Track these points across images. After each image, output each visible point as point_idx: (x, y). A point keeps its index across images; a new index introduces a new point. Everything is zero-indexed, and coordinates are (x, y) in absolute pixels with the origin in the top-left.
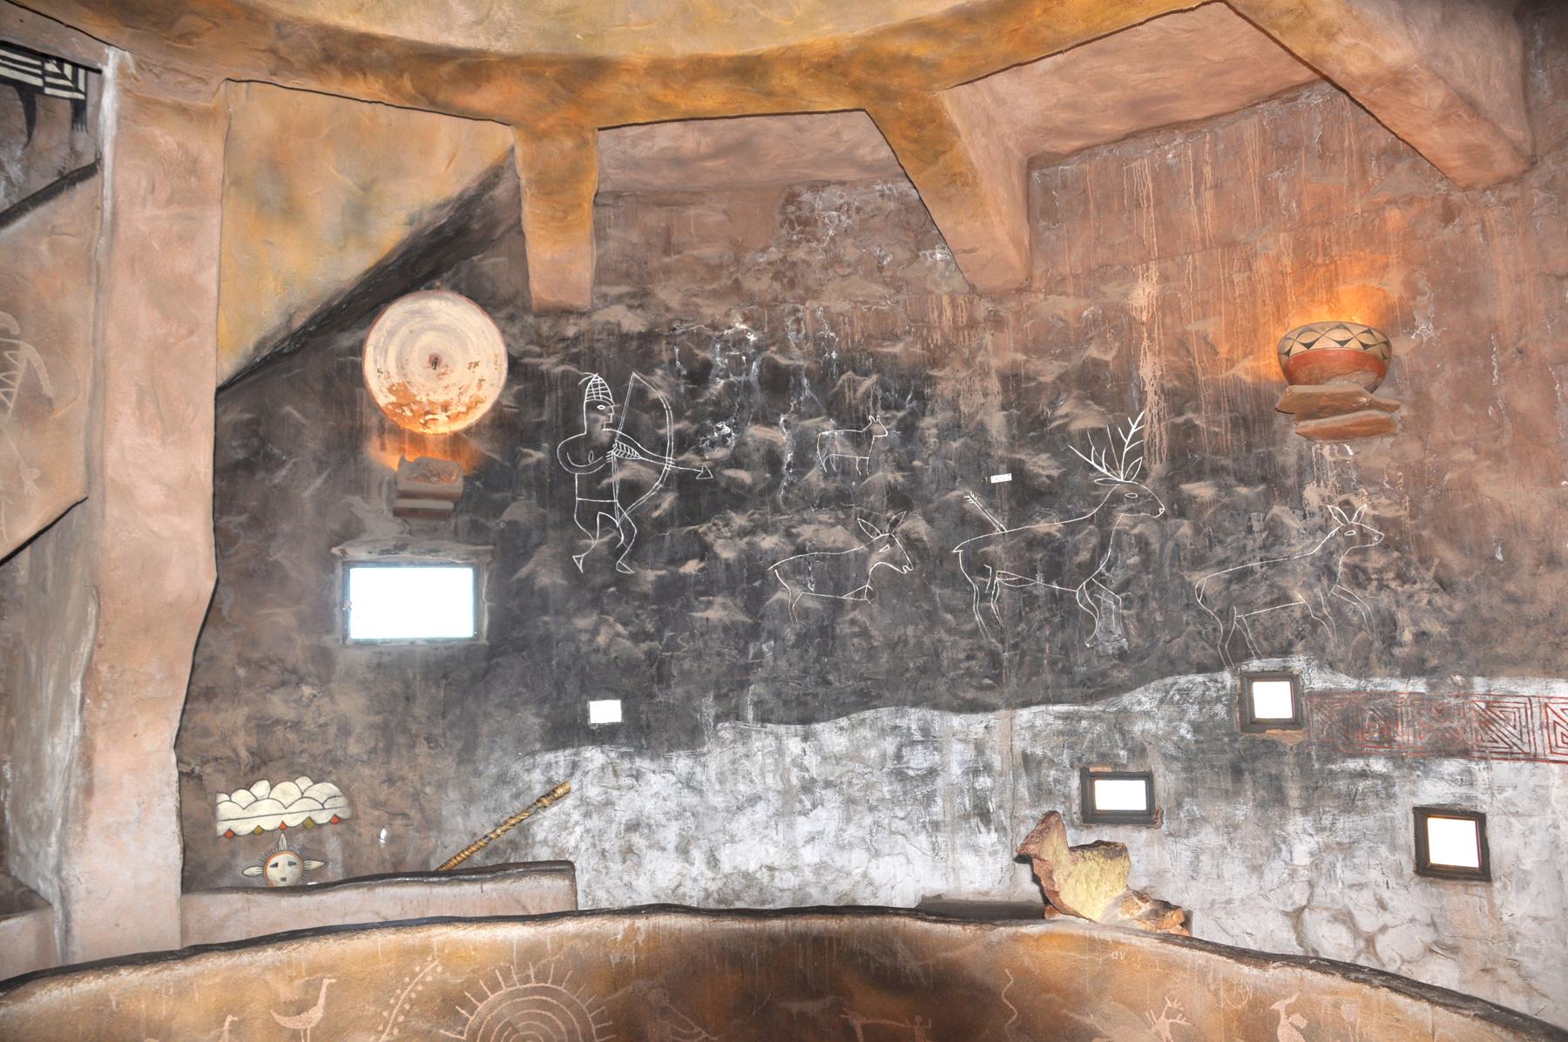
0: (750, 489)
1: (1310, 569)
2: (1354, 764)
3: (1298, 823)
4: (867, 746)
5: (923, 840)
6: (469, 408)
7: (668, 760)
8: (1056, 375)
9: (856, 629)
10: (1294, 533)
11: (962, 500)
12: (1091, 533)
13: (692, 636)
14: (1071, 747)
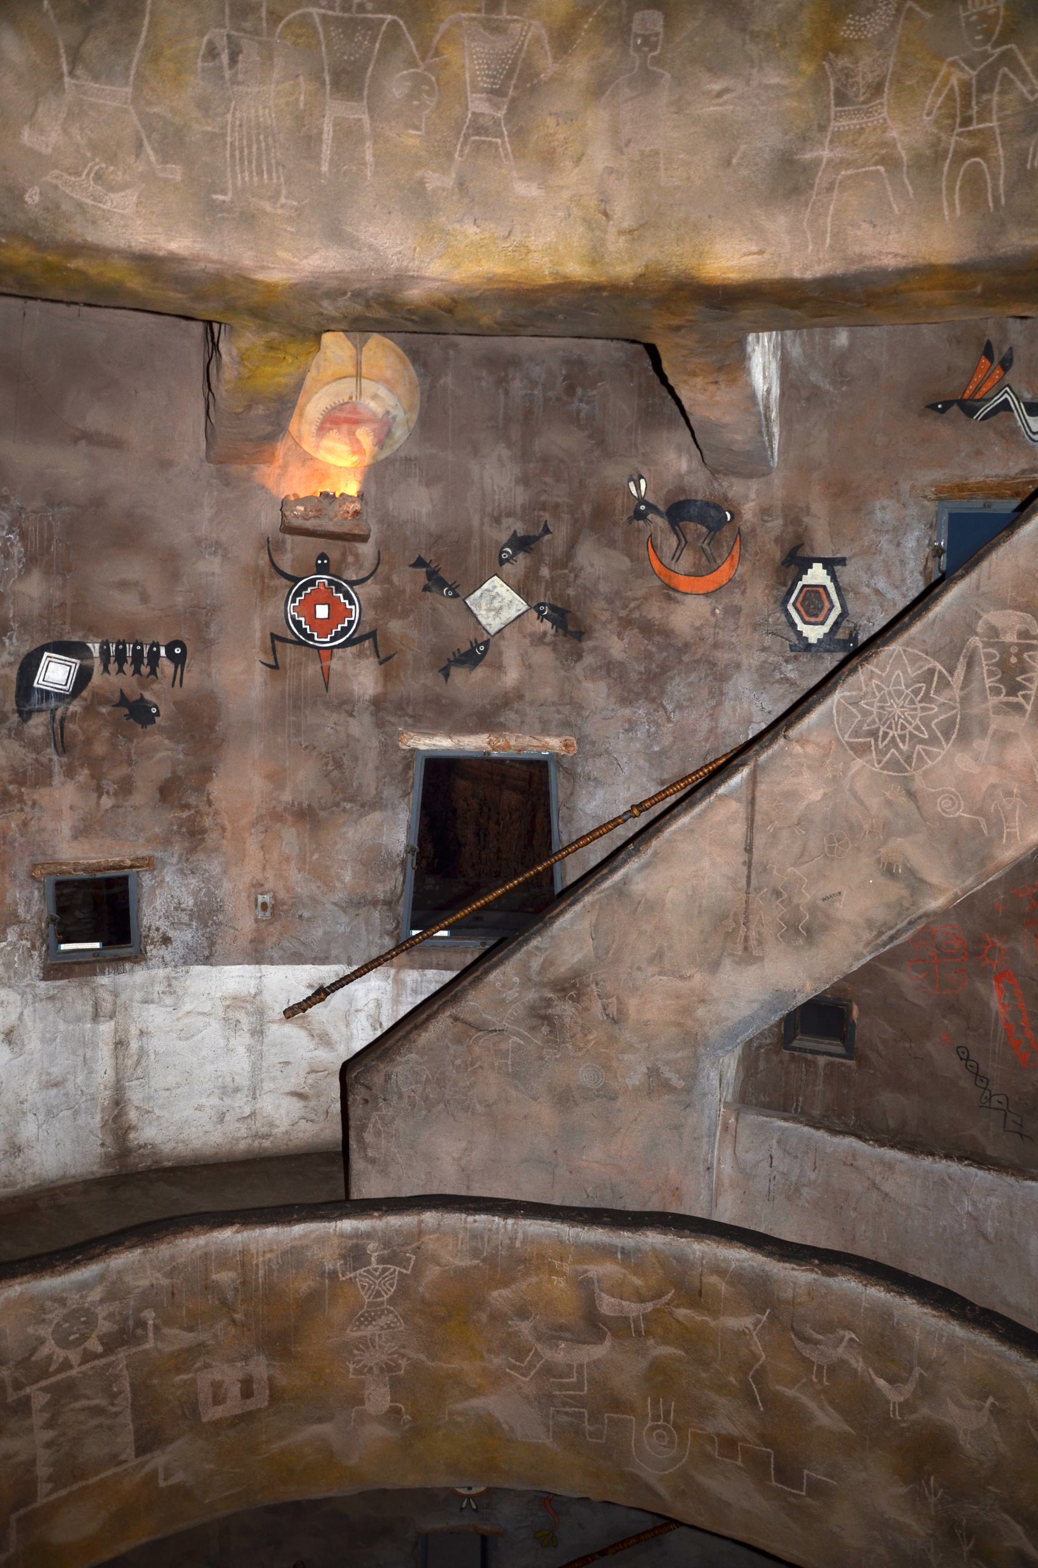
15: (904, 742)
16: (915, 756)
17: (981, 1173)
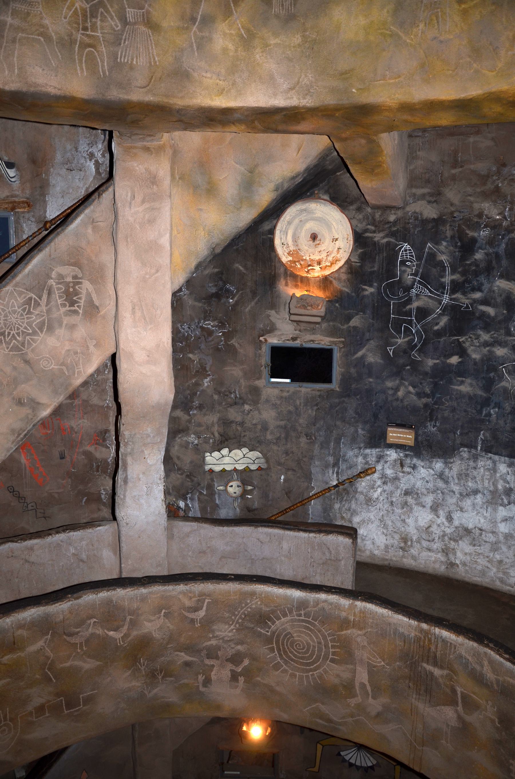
0: (493, 319)
6: (332, 264)
7: (431, 462)
15: (19, 336)
16: (26, 342)
17: (75, 533)
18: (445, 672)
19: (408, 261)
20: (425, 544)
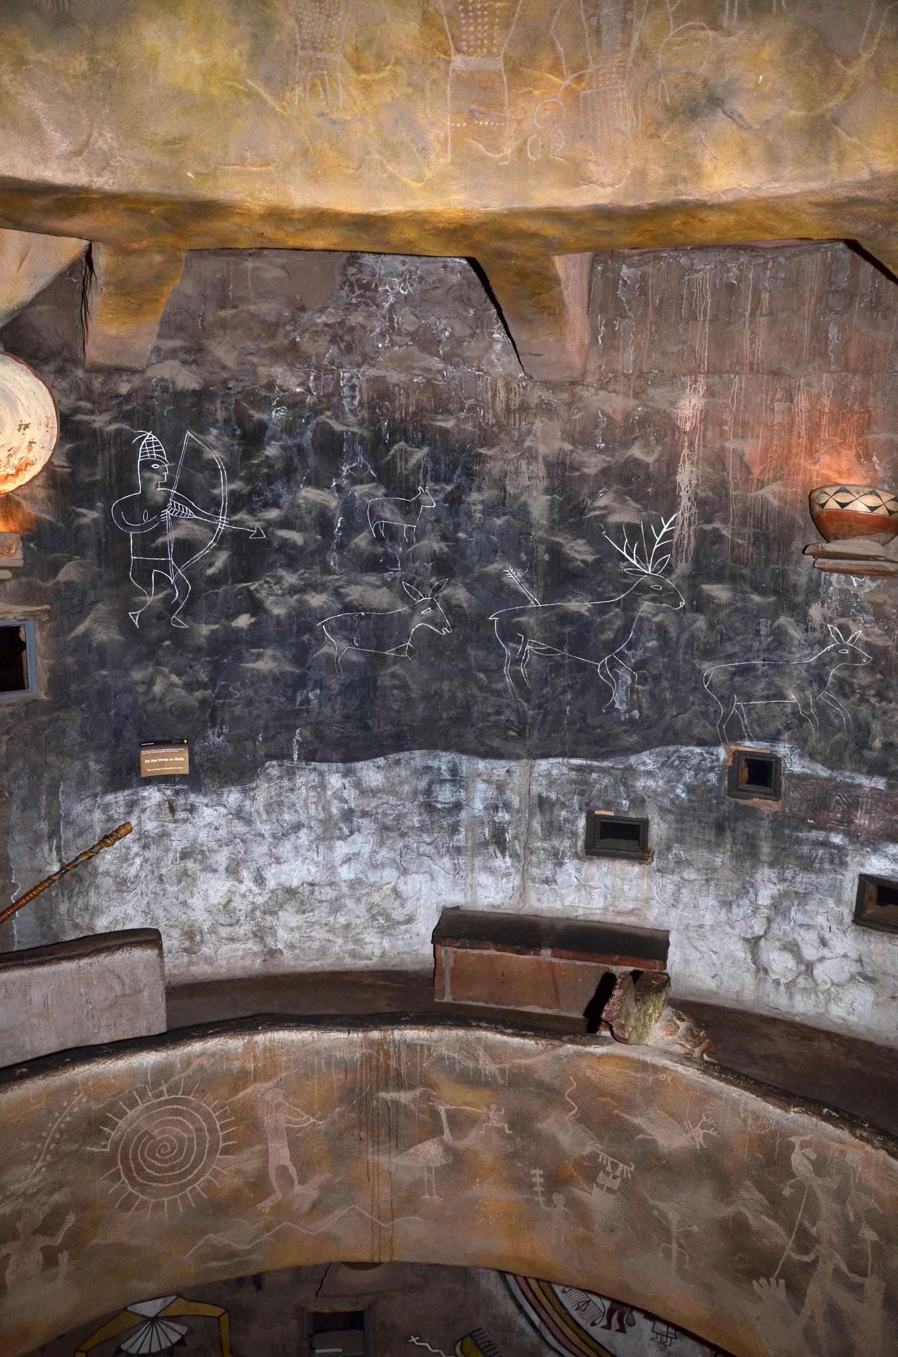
1: (804, 674)
2: (820, 835)
3: (765, 873)
4: (401, 783)
5: (446, 861)
6: (18, 470)
7: (220, 795)
8: (599, 468)
9: (397, 682)
10: (796, 642)
11: (501, 574)
12: (616, 615)
13: (243, 685)
14: (582, 793)
18: (418, 1092)
19: (155, 462)
20: (224, 932)
